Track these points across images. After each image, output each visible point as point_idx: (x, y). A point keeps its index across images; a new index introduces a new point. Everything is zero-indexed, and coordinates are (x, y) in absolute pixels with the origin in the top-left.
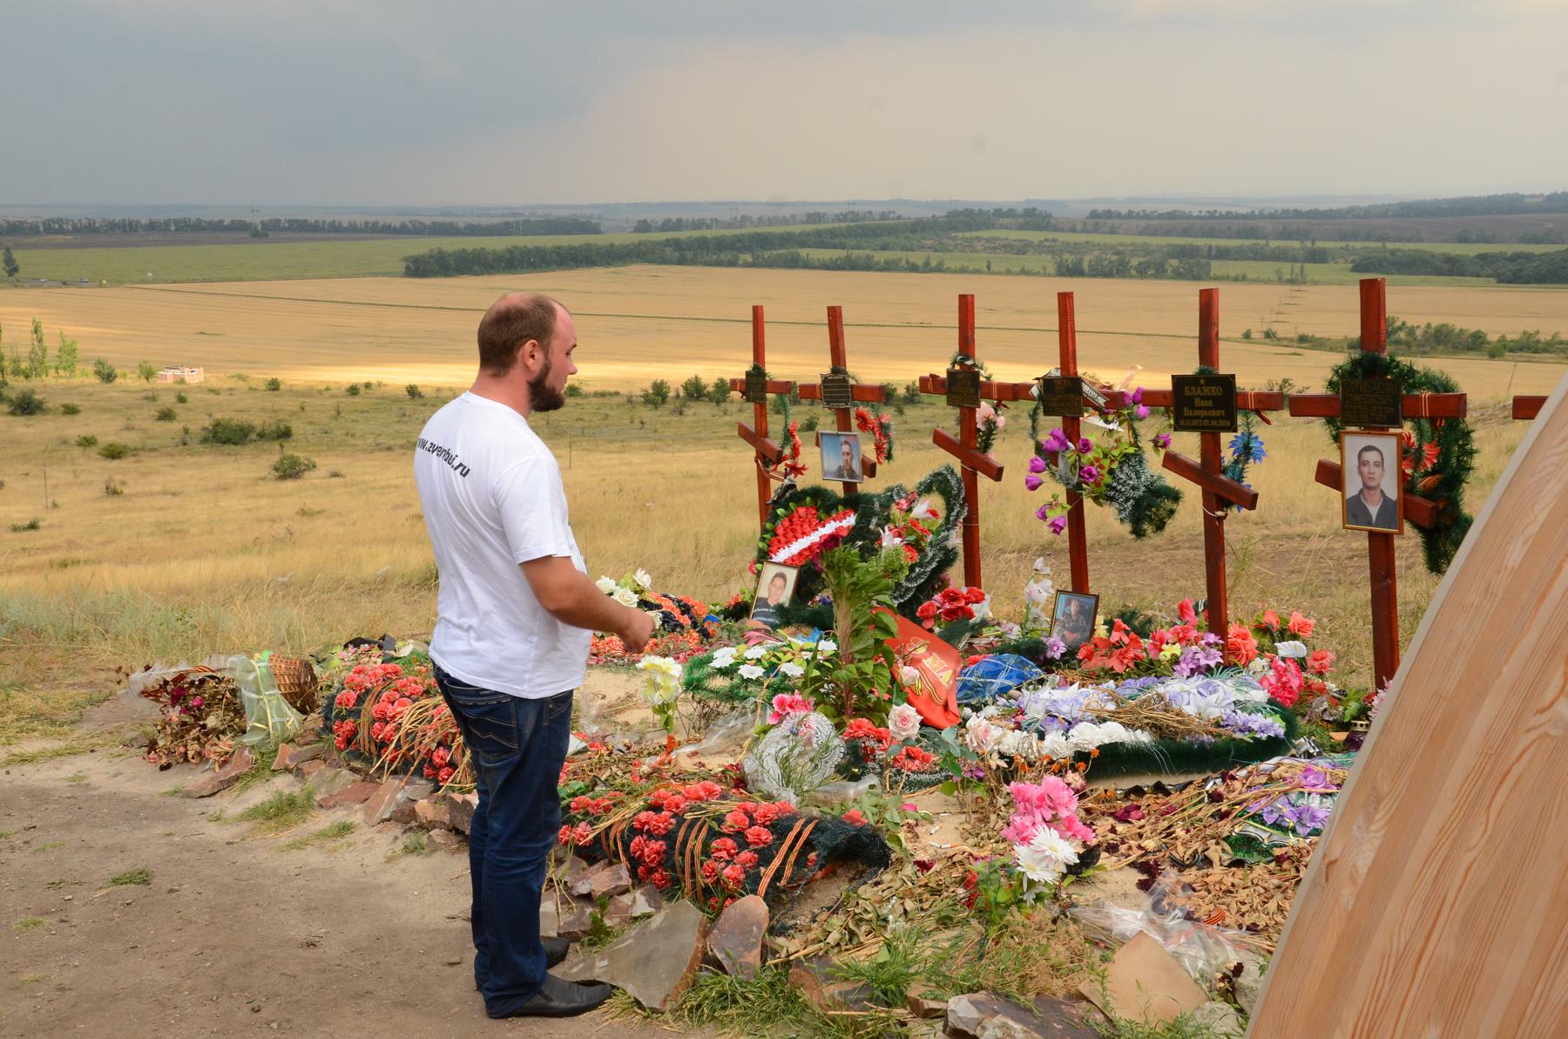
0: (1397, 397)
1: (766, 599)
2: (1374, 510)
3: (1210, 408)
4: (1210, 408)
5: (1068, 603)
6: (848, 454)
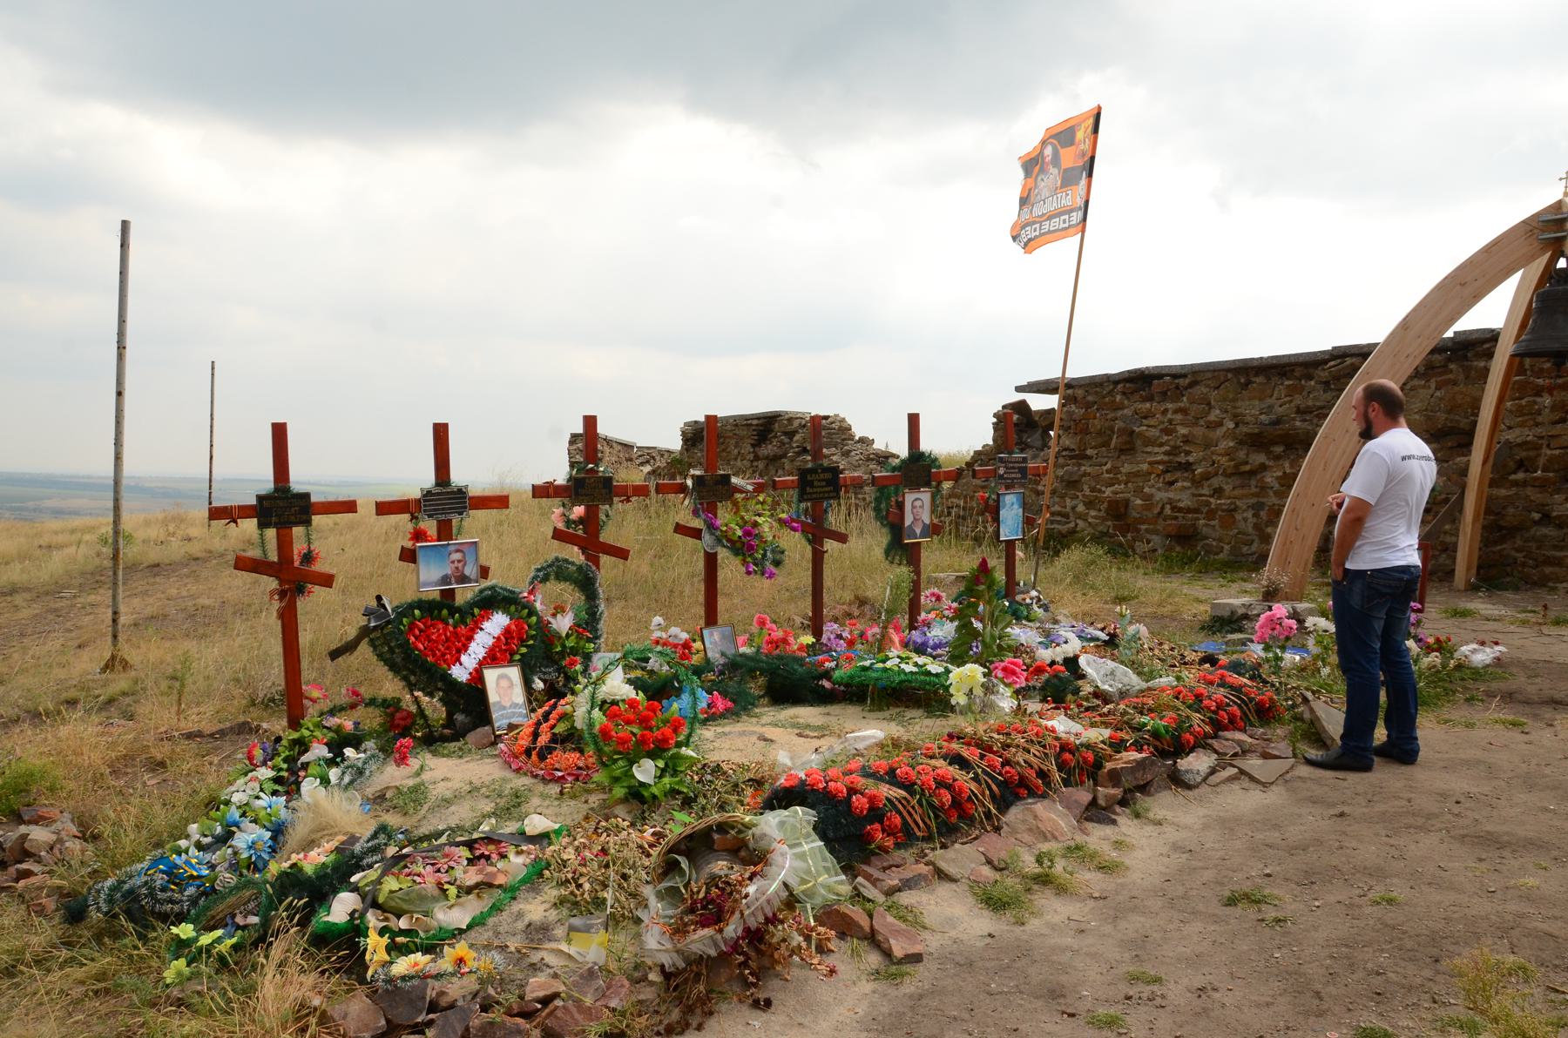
0: (930, 471)
1: (499, 702)
2: (918, 531)
3: (822, 487)
4: (822, 487)
5: (711, 634)
6: (459, 561)
